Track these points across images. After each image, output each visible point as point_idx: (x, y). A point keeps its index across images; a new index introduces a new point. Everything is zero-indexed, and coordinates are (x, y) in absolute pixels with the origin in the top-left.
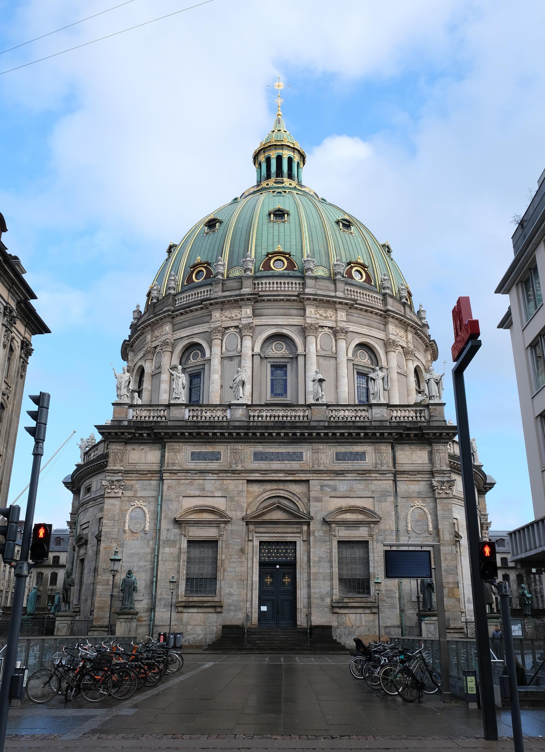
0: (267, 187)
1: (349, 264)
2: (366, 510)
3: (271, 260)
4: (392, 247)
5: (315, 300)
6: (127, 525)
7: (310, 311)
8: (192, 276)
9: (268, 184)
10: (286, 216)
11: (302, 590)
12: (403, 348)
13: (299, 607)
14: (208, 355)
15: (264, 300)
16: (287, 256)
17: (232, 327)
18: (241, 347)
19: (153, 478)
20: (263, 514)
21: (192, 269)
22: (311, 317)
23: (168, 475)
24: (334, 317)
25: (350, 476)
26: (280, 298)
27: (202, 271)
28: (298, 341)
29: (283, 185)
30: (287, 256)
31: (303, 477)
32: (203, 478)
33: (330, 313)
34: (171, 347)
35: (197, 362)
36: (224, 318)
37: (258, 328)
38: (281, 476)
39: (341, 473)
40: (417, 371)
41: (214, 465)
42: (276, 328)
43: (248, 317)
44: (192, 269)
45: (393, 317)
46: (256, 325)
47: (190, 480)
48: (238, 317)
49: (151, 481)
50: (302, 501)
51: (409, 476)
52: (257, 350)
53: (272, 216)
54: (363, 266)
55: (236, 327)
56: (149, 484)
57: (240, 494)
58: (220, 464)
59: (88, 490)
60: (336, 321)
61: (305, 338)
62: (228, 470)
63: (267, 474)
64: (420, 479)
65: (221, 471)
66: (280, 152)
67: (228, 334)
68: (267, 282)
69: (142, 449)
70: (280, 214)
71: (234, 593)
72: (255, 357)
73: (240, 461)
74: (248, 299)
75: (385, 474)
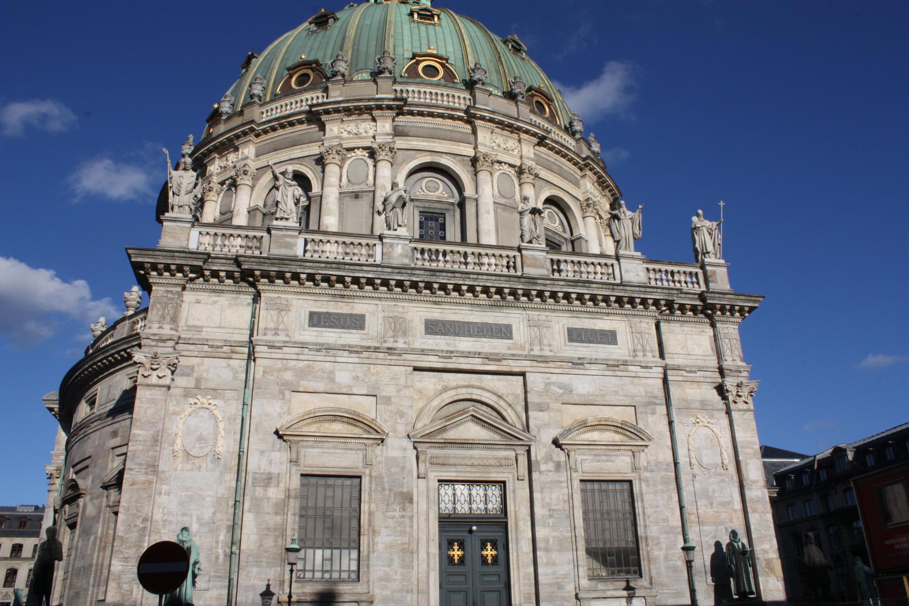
2: (626, 425)
3: (418, 64)
5: (491, 120)
6: (178, 441)
10: (436, 19)
11: (521, 570)
13: (517, 603)
14: (316, 189)
17: (358, 148)
19: (234, 356)
20: (443, 429)
22: (485, 145)
23: (265, 349)
24: (516, 152)
25: (594, 369)
27: (308, 76)
31: (516, 366)
32: (332, 359)
33: (512, 143)
34: (250, 179)
36: (345, 135)
37: (400, 152)
38: (476, 364)
39: (578, 363)
41: (352, 337)
42: (430, 155)
43: (388, 134)
45: (591, 170)
46: (398, 149)
47: (306, 362)
49: (231, 362)
50: (513, 409)
51: (684, 373)
53: (416, 16)
56: (225, 365)
57: (401, 392)
58: (363, 336)
60: (521, 157)
61: (476, 175)
62: (378, 348)
63: (450, 357)
64: (702, 380)
65: (367, 348)
67: (351, 160)
68: (416, 89)
69: (216, 302)
71: (394, 577)
73: (400, 332)
74: (389, 108)
75: (651, 368)
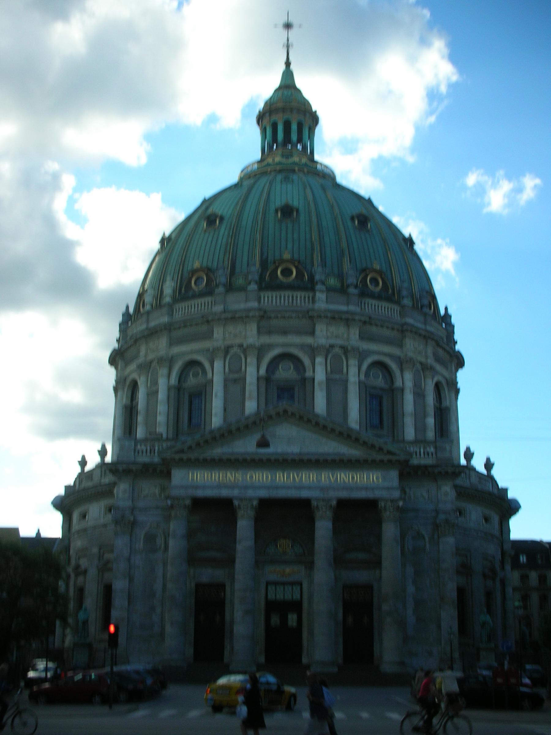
1: (364, 270)
7: (321, 328)
12: (421, 363)
24: (345, 336)
28: (306, 361)
40: (438, 386)
52: (263, 371)
54: (380, 273)
55: (241, 346)
59: (84, 516)
66: (287, 116)
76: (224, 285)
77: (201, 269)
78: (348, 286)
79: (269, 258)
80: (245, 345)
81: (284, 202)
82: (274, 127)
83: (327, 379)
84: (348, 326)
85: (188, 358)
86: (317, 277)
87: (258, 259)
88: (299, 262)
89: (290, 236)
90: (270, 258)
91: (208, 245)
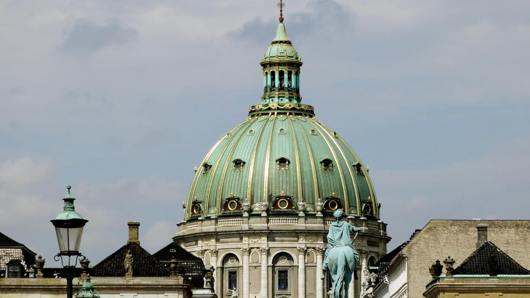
0: (272, 108)
1: (327, 198)
4: (361, 163)
8: (227, 205)
9: (273, 106)
10: (287, 163)
12: (360, 250)
15: (274, 233)
16: (288, 199)
17: (255, 248)
18: (261, 261)
21: (227, 201)
26: (284, 232)
27: (234, 202)
28: (294, 256)
29: (284, 107)
30: (288, 199)
35: (233, 264)
36: (251, 242)
42: (281, 249)
44: (227, 201)
48: (259, 242)
52: (270, 263)
53: (278, 163)
54: (336, 199)
55: (258, 248)
66: (281, 68)
70: (282, 161)
72: (269, 267)
76: (248, 212)
77: (233, 198)
78: (318, 211)
79: (273, 195)
80: (260, 249)
81: (281, 156)
82: (273, 73)
83: (305, 266)
84: (317, 236)
85: (228, 252)
86: (300, 208)
87: (265, 196)
88: (290, 198)
89: (284, 179)
90: (274, 195)
91: (237, 182)
